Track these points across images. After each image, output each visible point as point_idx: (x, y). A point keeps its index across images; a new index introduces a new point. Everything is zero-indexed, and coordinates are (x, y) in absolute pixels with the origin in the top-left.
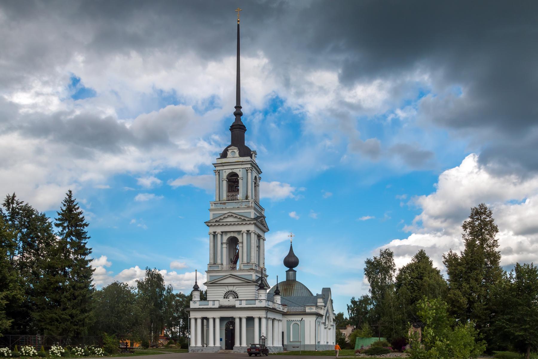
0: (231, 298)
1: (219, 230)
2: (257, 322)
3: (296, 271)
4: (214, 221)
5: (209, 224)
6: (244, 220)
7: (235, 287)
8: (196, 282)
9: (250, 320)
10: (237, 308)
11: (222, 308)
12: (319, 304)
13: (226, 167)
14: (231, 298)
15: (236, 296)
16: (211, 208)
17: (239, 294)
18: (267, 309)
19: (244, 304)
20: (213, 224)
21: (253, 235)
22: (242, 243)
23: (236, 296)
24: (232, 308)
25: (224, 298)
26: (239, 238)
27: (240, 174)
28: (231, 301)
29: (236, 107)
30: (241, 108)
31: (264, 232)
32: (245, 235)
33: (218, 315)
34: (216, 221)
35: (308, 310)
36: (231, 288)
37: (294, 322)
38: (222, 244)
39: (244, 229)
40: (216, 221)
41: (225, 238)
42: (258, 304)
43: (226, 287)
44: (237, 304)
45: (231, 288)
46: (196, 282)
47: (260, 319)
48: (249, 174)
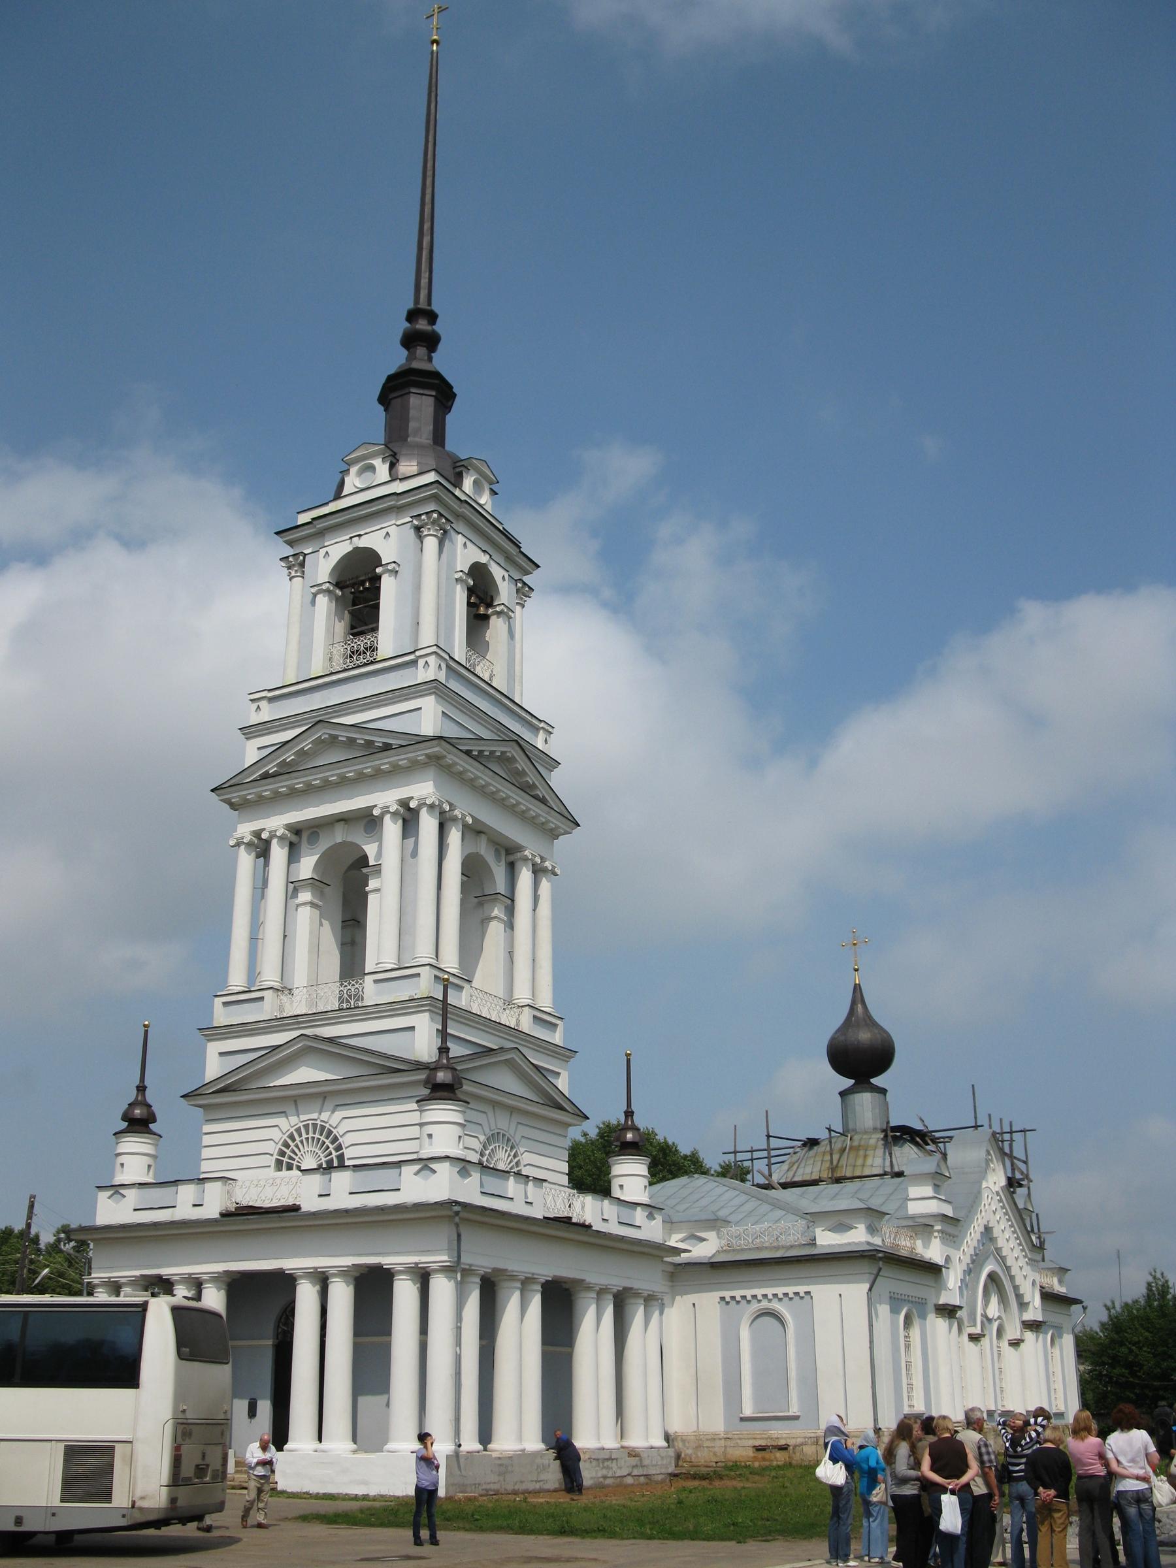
1: (276, 822)
2: (405, 1293)
3: (883, 1091)
5: (235, 796)
6: (387, 747)
8: (141, 1089)
9: (373, 1288)
11: (245, 1219)
12: (914, 1208)
16: (255, 719)
18: (455, 1215)
21: (424, 815)
25: (279, 1165)
29: (412, 316)
30: (432, 317)
31: (554, 834)
32: (392, 829)
34: (266, 776)
35: (827, 1240)
37: (755, 1306)
46: (141, 1089)
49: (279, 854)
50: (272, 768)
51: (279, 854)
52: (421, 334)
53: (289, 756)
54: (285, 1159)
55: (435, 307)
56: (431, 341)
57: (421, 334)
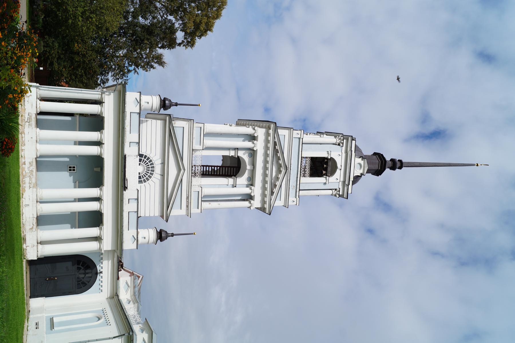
0: (141, 169)
2: (94, 231)
4: (276, 140)
7: (159, 177)
10: (122, 195)
13: (344, 155)
14: (141, 169)
15: (142, 179)
17: (146, 184)
19: (128, 207)
20: (271, 138)
22: (234, 186)
23: (142, 179)
24: (122, 184)
26: (242, 180)
27: (332, 179)
28: (134, 167)
30: (400, 168)
33: (108, 155)
36: (158, 169)
38: (237, 149)
39: (257, 191)
40: (275, 144)
41: (244, 156)
42: (128, 235)
43: (160, 161)
44: (127, 194)
45: (158, 169)
47: (98, 239)
48: (330, 192)
49: (249, 144)
50: (277, 147)
51: (249, 144)
52: (396, 165)
53: (279, 154)
54: (143, 159)
55: (404, 168)
56: (393, 168)
57: (396, 165)
